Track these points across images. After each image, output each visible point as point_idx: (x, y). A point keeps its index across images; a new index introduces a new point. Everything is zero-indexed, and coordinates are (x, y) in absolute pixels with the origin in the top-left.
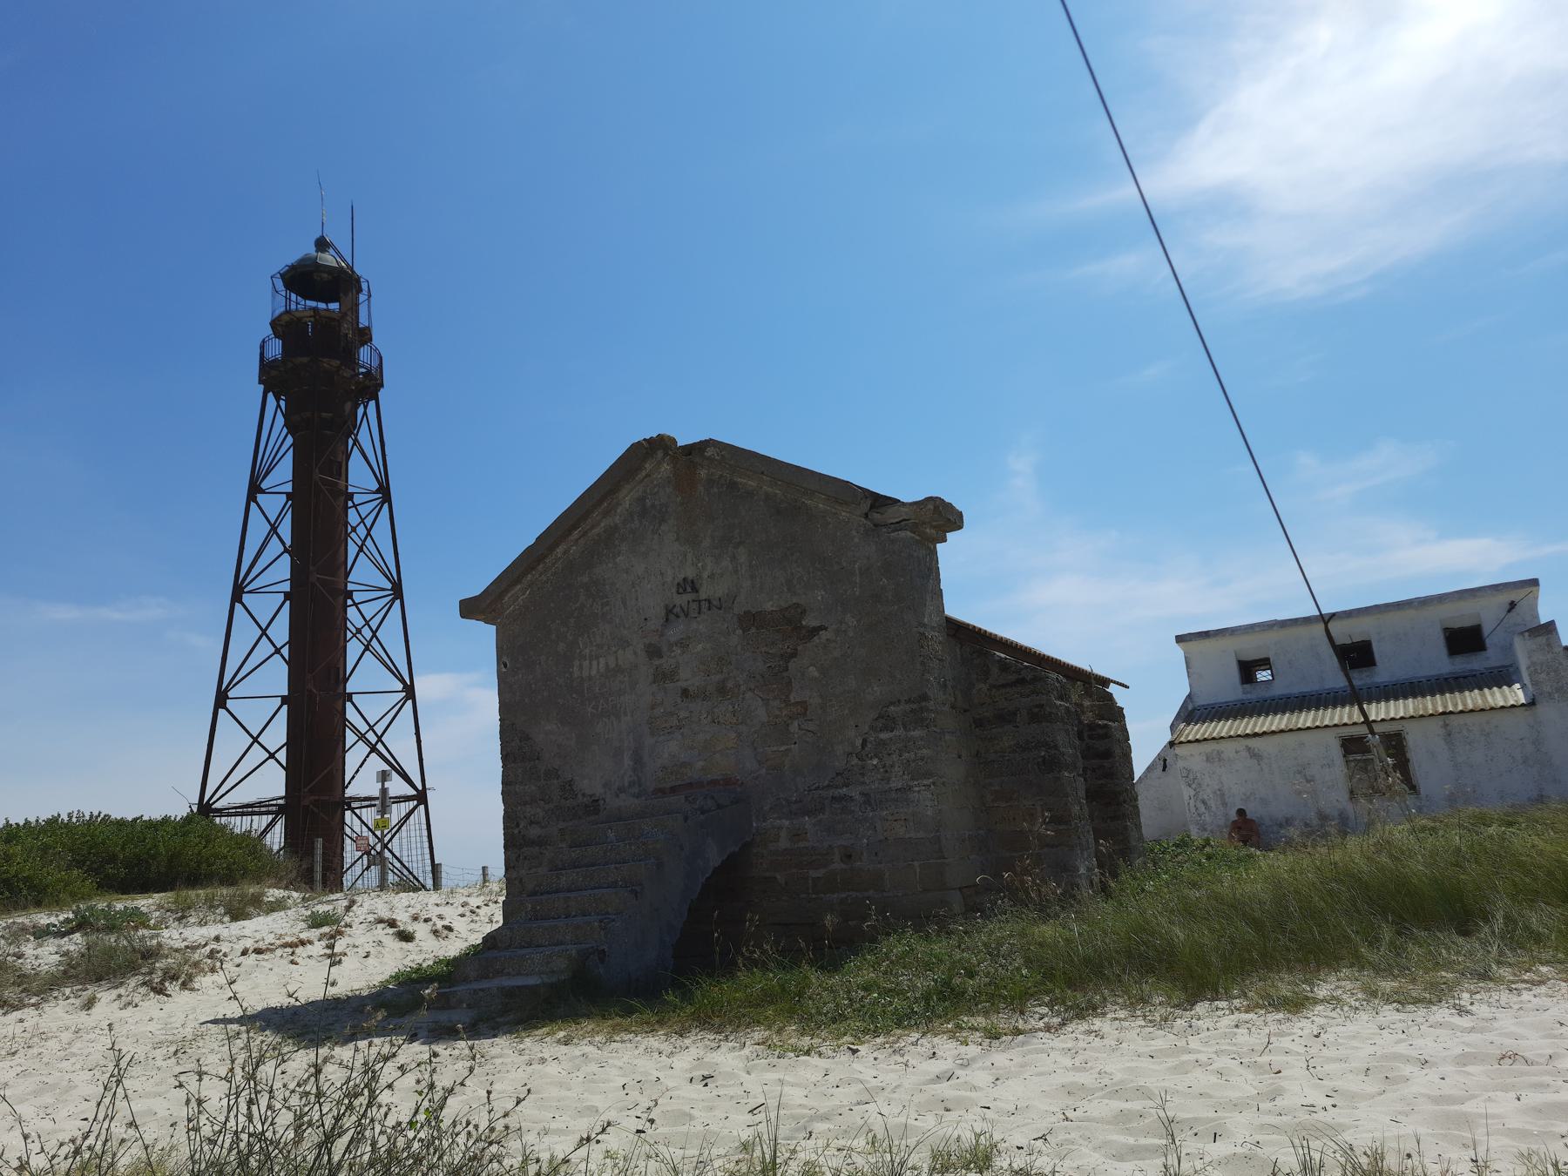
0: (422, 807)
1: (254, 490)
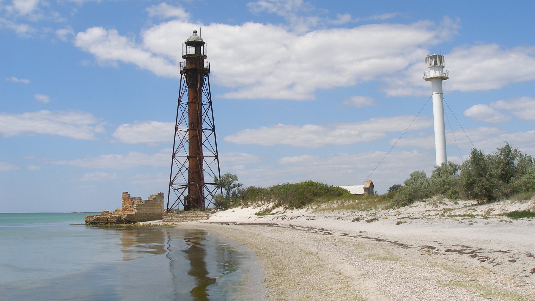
1: (180, 101)
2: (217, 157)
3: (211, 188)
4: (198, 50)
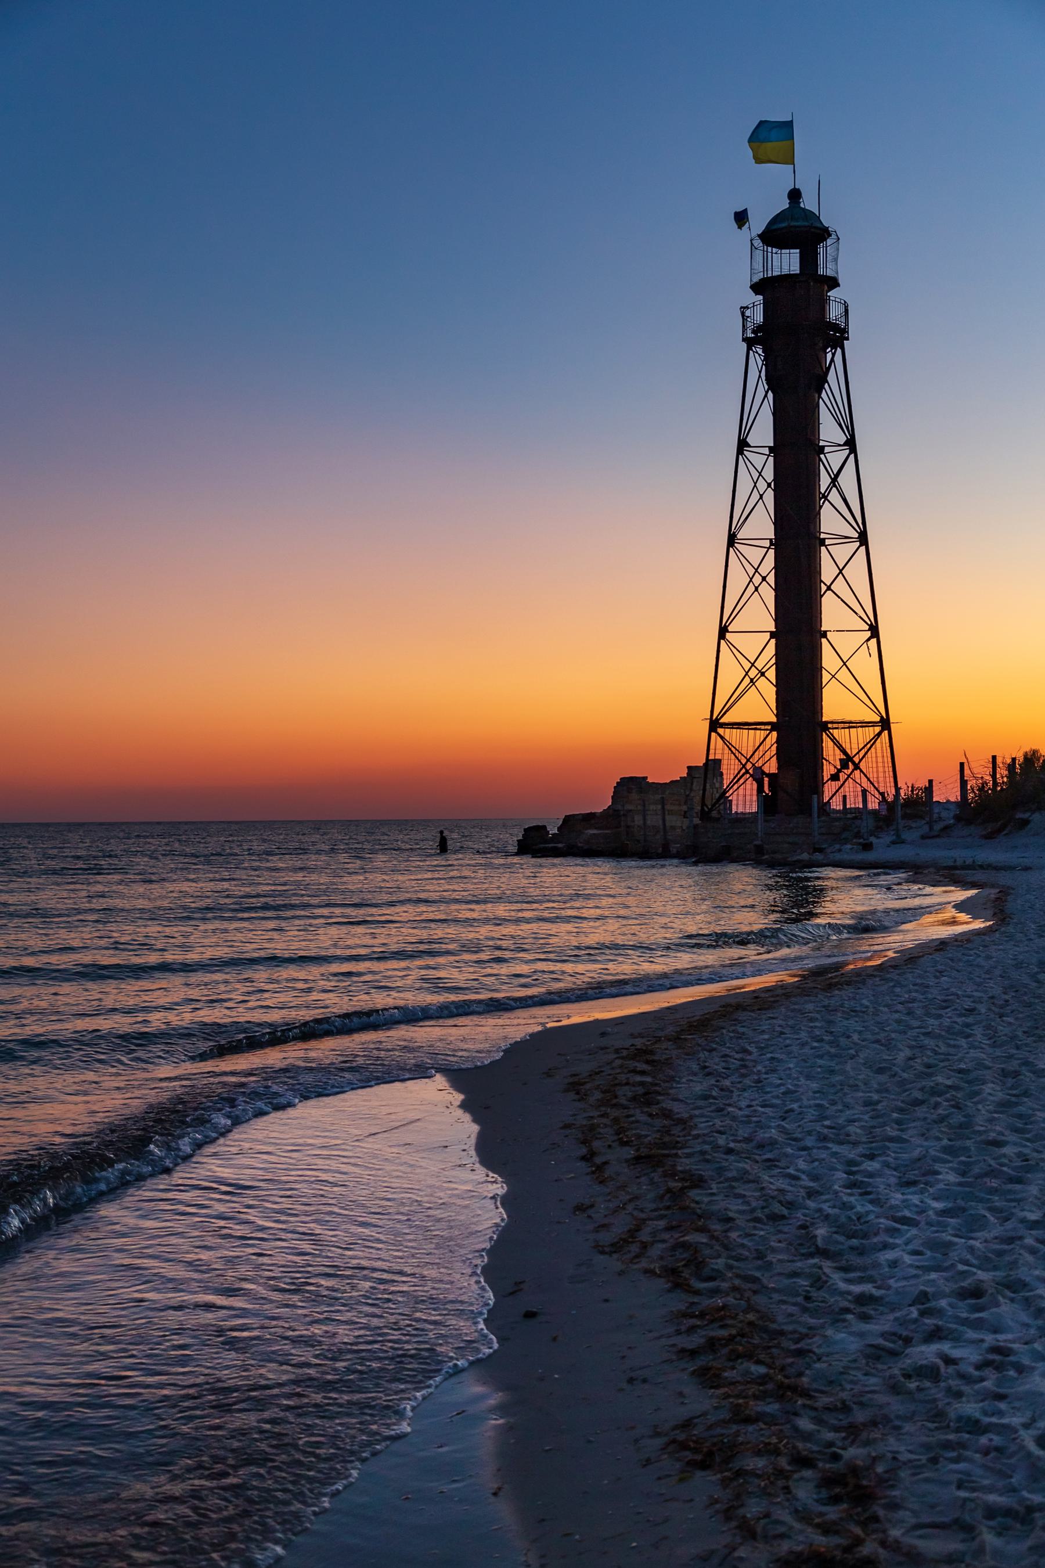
0: (886, 732)
1: (742, 445)
2: (874, 631)
4: (809, 260)
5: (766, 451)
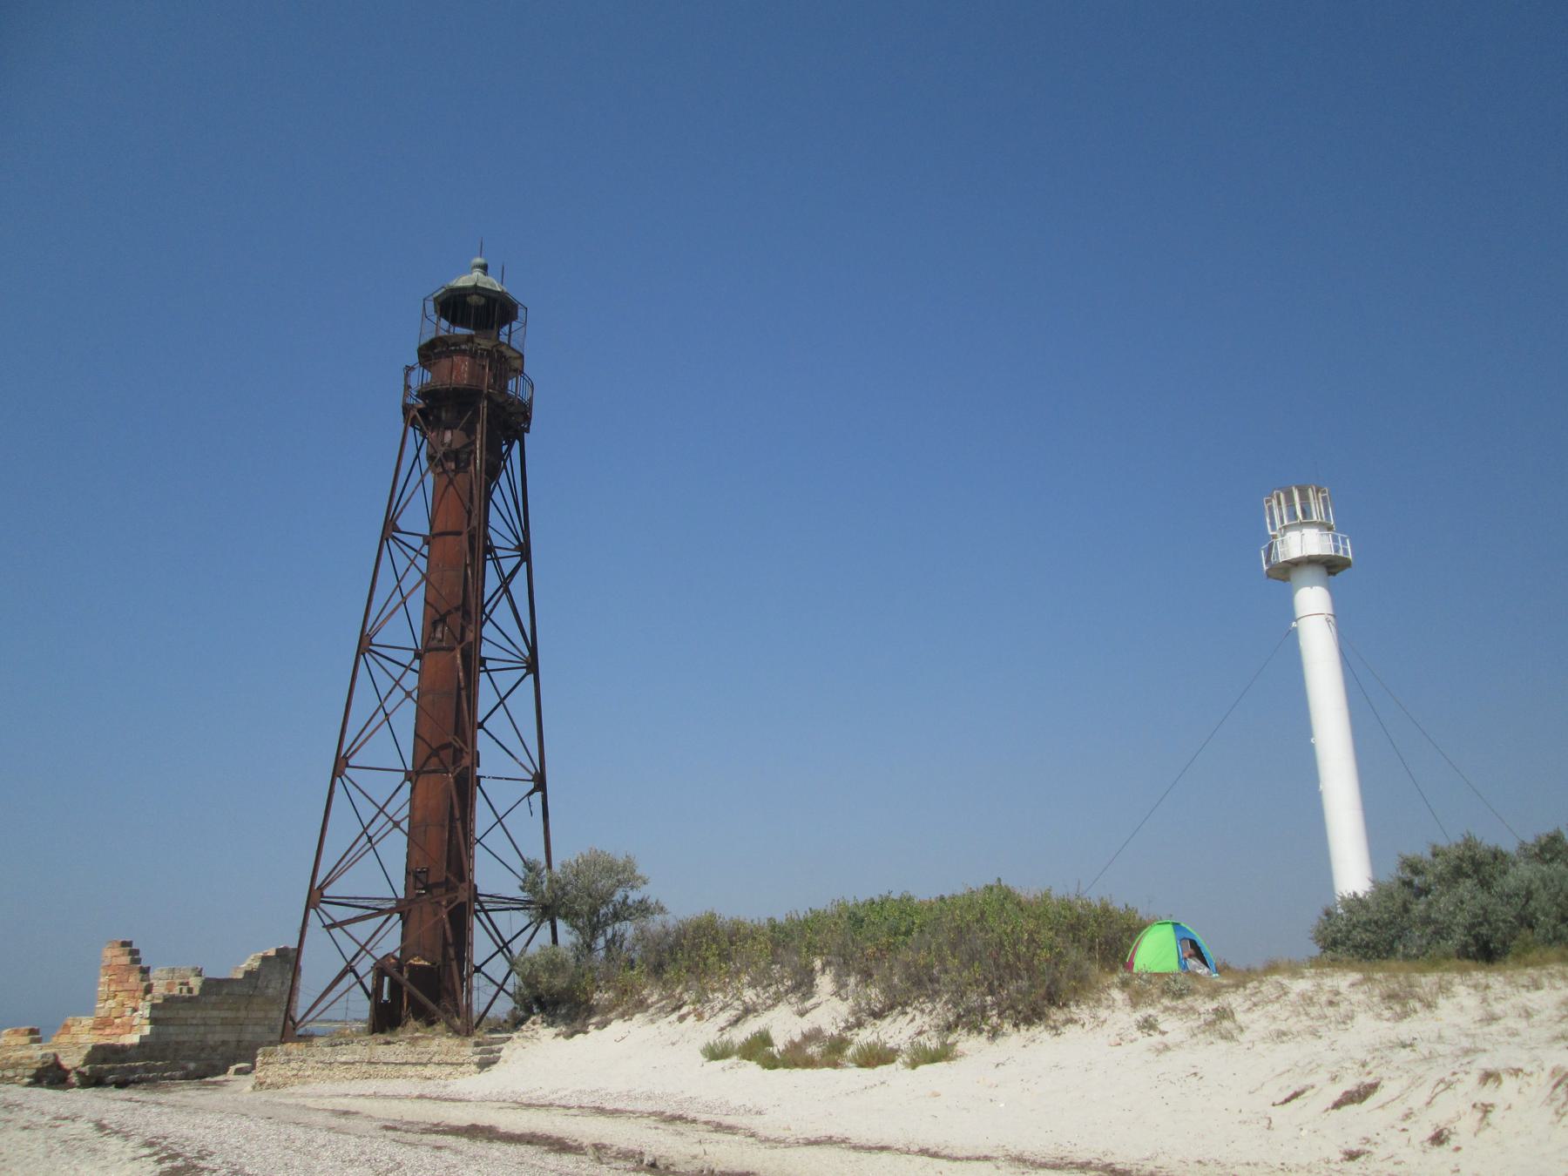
1: (390, 528)
2: (540, 782)
3: (510, 922)
5: (417, 542)
